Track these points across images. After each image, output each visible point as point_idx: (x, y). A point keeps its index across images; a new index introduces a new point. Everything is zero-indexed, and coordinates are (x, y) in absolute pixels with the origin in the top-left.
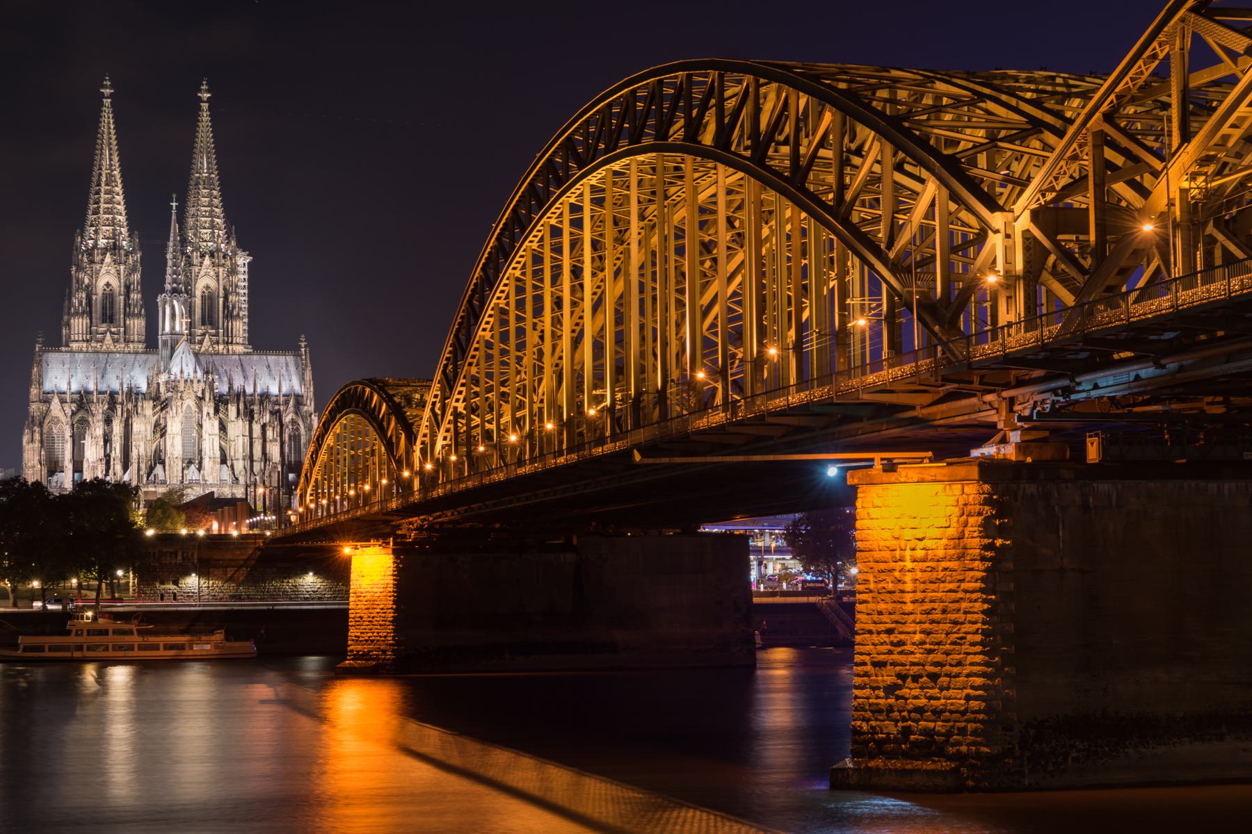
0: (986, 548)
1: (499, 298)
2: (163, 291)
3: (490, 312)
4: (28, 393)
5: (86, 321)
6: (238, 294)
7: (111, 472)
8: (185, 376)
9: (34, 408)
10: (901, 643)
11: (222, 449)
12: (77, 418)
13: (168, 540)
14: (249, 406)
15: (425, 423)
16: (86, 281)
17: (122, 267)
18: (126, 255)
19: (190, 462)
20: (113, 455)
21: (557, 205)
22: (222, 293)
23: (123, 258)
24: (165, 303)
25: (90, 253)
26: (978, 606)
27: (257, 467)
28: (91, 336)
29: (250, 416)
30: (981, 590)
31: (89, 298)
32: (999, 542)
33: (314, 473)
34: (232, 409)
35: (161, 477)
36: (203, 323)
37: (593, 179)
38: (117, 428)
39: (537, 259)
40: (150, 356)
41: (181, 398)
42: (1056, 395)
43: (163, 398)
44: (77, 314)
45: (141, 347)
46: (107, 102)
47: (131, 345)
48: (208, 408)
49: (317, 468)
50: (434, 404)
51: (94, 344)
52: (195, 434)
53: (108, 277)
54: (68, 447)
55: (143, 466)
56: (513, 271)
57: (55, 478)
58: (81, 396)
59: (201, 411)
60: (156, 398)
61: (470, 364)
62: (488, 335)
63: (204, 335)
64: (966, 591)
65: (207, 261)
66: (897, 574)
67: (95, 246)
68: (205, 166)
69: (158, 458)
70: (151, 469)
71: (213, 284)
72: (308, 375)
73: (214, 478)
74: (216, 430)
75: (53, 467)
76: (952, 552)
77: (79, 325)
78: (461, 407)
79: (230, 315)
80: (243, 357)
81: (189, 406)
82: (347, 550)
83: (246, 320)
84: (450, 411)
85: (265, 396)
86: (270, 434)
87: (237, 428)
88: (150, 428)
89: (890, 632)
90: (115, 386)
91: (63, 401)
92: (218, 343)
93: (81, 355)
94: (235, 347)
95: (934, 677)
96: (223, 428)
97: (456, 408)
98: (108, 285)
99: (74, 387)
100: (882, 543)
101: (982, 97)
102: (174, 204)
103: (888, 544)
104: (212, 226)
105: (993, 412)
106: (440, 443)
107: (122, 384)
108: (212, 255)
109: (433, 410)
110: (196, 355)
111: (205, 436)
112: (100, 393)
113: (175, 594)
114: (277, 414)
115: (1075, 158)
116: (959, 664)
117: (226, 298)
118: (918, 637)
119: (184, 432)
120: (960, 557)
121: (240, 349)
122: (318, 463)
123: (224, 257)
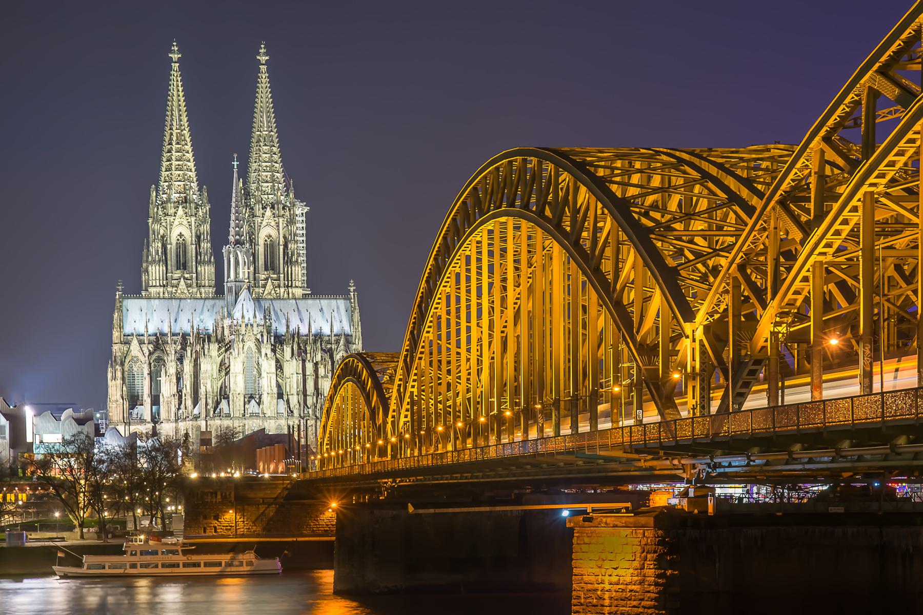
0: (658, 576)
1: (436, 308)
2: (227, 242)
3: (430, 319)
4: (112, 334)
5: (162, 268)
6: (296, 242)
7: (182, 406)
8: (246, 321)
9: (115, 348)
11: (279, 386)
12: (154, 357)
14: (303, 345)
16: (162, 232)
17: (193, 219)
18: (196, 208)
19: (251, 397)
20: (184, 391)
21: (467, 242)
22: (282, 240)
23: (194, 211)
24: (229, 253)
27: (310, 401)
29: (301, 354)
30: (654, 607)
31: (164, 247)
32: (669, 572)
33: (329, 427)
34: (287, 350)
35: (226, 411)
36: (266, 269)
37: (490, 225)
38: (188, 367)
40: (217, 301)
41: (243, 341)
42: (710, 467)
43: (227, 341)
44: (154, 261)
45: (212, 290)
47: (202, 290)
48: (266, 349)
49: (330, 423)
50: (399, 386)
51: (169, 289)
52: (255, 373)
53: (179, 226)
54: (147, 382)
55: (210, 401)
57: (135, 411)
58: (157, 338)
59: (260, 352)
60: (220, 341)
61: (420, 359)
63: (267, 279)
64: (644, 607)
65: (268, 212)
66: (599, 593)
67: (169, 200)
69: (223, 394)
70: (218, 403)
71: (274, 233)
74: (274, 370)
76: (636, 578)
77: (155, 272)
78: (415, 390)
79: (289, 262)
80: (300, 303)
81: (249, 347)
83: (305, 265)
84: (408, 395)
85: (319, 337)
86: (322, 371)
87: (292, 367)
88: (216, 368)
90: (187, 328)
91: (141, 343)
92: (279, 286)
93: (157, 301)
94: (294, 290)
96: (279, 367)
97: (412, 393)
98: (181, 235)
99: (151, 330)
100: (590, 570)
102: (235, 163)
103: (593, 571)
104: (273, 181)
105: (681, 471)
106: (402, 420)
107: (193, 327)
108: (273, 207)
109: (399, 390)
110: (258, 300)
111: (264, 374)
112: (174, 335)
113: (215, 528)
114: (330, 353)
117: (286, 246)
120: (641, 583)
122: (331, 419)
123: (284, 208)
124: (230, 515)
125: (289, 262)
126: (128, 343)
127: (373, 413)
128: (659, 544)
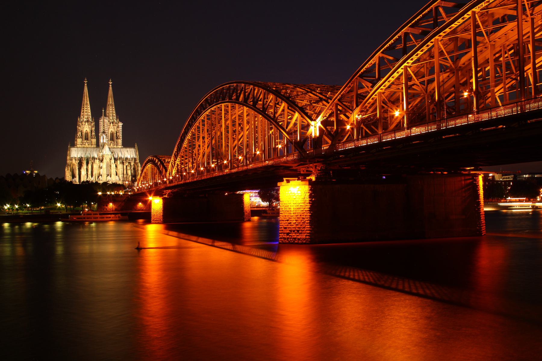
9: (68, 161)
10: (290, 223)
13: (104, 195)
15: (170, 167)
19: (108, 175)
25: (82, 122)
26: (308, 214)
27: (125, 176)
28: (82, 143)
29: (123, 163)
34: (119, 162)
39: (198, 127)
45: (95, 146)
46: (86, 84)
48: (113, 161)
53: (86, 128)
56: (193, 130)
60: (99, 159)
62: (186, 146)
65: (112, 124)
68: (111, 100)
71: (113, 130)
72: (137, 153)
73: (114, 179)
75: (73, 176)
77: (79, 141)
78: (179, 163)
79: (117, 138)
82: (150, 198)
84: (176, 164)
85: (127, 159)
86: (128, 168)
87: (120, 166)
89: (288, 220)
91: (76, 160)
95: (298, 231)
96: (116, 166)
99: (79, 156)
101: (308, 92)
106: (174, 172)
115: (331, 109)
116: (304, 228)
118: (294, 222)
119: (107, 167)
121: (120, 147)
124: (111, 205)
125: (117, 138)
126: (72, 160)
127: (161, 172)
128: (310, 190)
